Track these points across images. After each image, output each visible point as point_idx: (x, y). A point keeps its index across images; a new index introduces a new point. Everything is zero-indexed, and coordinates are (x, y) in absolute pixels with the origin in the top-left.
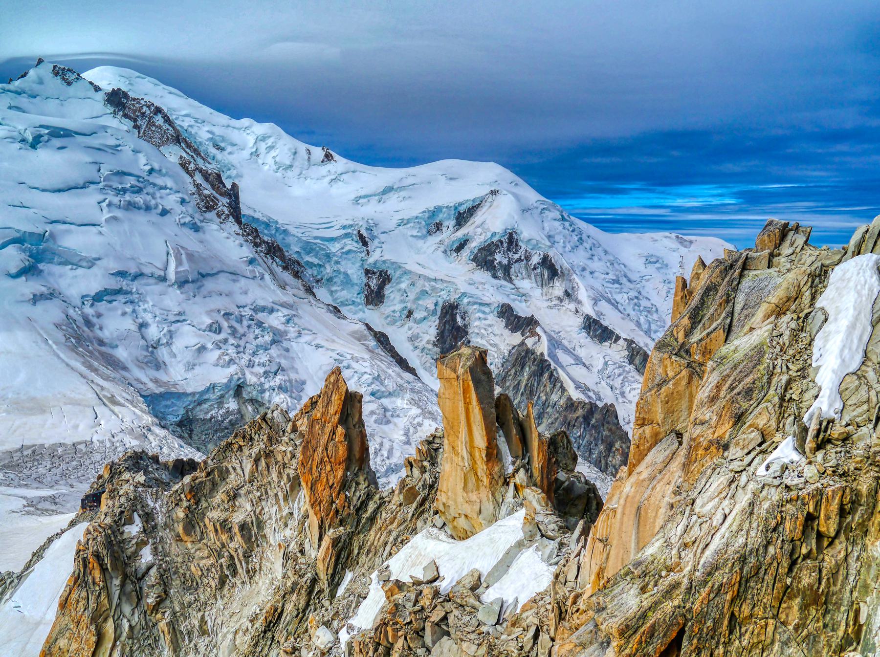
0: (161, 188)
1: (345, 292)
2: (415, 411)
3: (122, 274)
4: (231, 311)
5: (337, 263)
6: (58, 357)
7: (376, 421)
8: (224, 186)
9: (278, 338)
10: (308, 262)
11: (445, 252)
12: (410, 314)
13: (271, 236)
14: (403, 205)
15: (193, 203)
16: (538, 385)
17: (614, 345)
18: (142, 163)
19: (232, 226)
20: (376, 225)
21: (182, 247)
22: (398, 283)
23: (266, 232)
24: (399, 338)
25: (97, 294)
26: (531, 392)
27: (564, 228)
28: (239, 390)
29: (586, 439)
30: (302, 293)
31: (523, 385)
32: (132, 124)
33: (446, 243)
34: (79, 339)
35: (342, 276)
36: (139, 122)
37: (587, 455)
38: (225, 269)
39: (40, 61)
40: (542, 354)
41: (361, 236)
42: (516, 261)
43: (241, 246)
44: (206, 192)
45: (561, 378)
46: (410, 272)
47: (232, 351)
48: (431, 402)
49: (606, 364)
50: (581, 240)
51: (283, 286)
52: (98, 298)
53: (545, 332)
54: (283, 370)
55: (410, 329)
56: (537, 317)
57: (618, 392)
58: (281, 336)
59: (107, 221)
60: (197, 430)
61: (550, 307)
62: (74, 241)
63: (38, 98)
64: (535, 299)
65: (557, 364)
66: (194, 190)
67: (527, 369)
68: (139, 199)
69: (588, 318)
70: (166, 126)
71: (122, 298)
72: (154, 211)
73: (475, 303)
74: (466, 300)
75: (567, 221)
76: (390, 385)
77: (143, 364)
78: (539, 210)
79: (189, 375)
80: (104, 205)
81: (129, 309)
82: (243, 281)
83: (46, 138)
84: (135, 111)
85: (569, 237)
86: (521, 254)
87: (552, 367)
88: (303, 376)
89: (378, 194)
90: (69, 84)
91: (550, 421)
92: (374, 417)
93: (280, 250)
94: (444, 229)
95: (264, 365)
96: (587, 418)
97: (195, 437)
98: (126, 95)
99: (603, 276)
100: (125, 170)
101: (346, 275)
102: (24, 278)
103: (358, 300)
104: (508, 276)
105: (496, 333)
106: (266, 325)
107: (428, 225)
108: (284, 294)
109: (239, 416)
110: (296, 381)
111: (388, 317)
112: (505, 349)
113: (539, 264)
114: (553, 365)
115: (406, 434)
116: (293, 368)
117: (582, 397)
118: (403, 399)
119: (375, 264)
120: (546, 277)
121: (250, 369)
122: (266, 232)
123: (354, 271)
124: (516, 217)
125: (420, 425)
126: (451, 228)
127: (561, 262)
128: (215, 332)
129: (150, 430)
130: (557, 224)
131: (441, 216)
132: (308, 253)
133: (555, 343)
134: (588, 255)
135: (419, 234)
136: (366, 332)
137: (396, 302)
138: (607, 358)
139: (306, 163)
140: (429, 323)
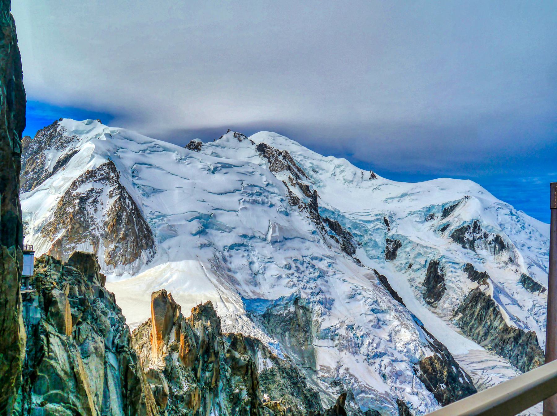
0: (272, 193)
1: (374, 251)
2: (396, 323)
3: (245, 236)
4: (298, 258)
5: (371, 235)
6: (206, 275)
7: (372, 326)
8: (310, 192)
9: (322, 275)
10: (354, 234)
11: (435, 231)
12: (410, 266)
13: (335, 218)
14: (413, 203)
15: (287, 201)
16: (486, 315)
17: (541, 294)
18: (264, 181)
19: (306, 214)
20: (395, 214)
21: (277, 224)
22: (405, 248)
23: (332, 216)
24: (399, 281)
25: (231, 246)
26: (481, 319)
27: (512, 220)
28: (296, 301)
29: (515, 353)
30: (340, 251)
31: (476, 314)
32: (268, 160)
33: (435, 226)
34: (218, 267)
35: (373, 242)
36: (271, 159)
37: (515, 362)
38: (299, 236)
39: (229, 131)
40: (489, 296)
41: (386, 220)
42: (478, 239)
43: (309, 224)
44: (294, 196)
45: (501, 312)
46: (412, 242)
47: (295, 280)
48: (407, 319)
49: (534, 305)
50: (523, 227)
51: (329, 247)
52: (231, 247)
53: (493, 282)
54: (322, 292)
55: (410, 275)
56: (489, 273)
57: (541, 324)
58: (324, 274)
59: (241, 209)
60: (272, 320)
61: (499, 268)
62: (225, 219)
63: (226, 148)
64: (489, 262)
65: (498, 302)
66: (288, 194)
67: (479, 304)
68: (259, 199)
69: (524, 276)
70: (283, 161)
71: (243, 248)
72: (266, 205)
73: (450, 262)
74: (444, 260)
75: (514, 215)
76: (384, 306)
77: (248, 283)
78: (496, 208)
79: (271, 291)
80: (241, 201)
81: (246, 254)
82: (308, 243)
83: (219, 168)
84: (269, 154)
85: (514, 226)
86: (482, 234)
87: (495, 305)
88: (333, 297)
89: (399, 197)
90: (241, 141)
91: (492, 338)
92: (372, 324)
93: (339, 226)
94: (435, 218)
95: (312, 289)
96: (516, 339)
97: (271, 324)
98: (266, 146)
99: (537, 250)
100: (255, 184)
101: (375, 242)
102: (198, 236)
103: (381, 256)
104: (472, 247)
105: (461, 281)
106: (316, 267)
107: (426, 215)
108: (330, 251)
109: (294, 315)
110: (329, 299)
111: (397, 267)
112: (467, 291)
113: (493, 241)
114: (496, 304)
115: (390, 336)
116: (329, 291)
117: (514, 325)
118: (390, 315)
119: (392, 236)
120: (497, 249)
121: (304, 290)
122: (332, 216)
123: (380, 240)
124: (479, 212)
125: (399, 331)
126: (440, 217)
127: (507, 240)
128: (288, 269)
129: (240, 317)
130: (507, 217)
131: (434, 210)
132: (355, 229)
133: (499, 290)
134: (528, 237)
135: (420, 220)
136: (374, 275)
137: (403, 258)
138: (535, 302)
139: (361, 180)
140: (422, 272)
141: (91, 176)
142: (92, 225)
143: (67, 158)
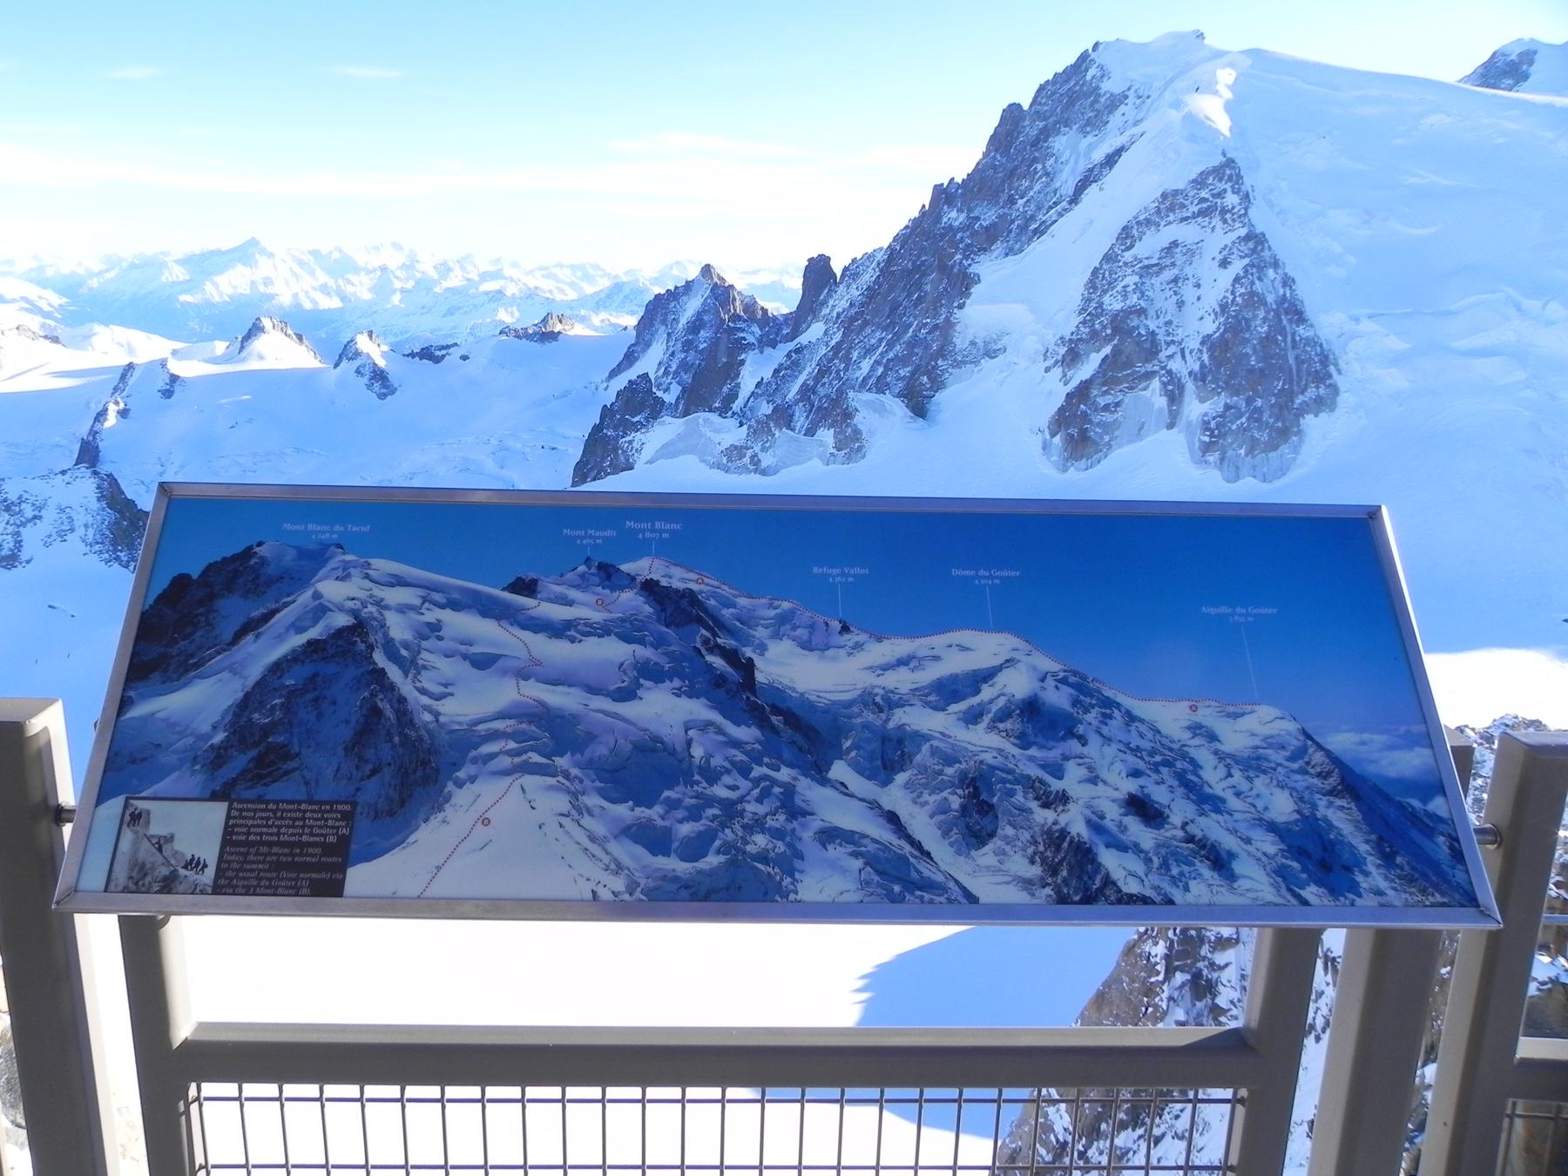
141: (1171, 209)
142: (1168, 344)
143: (1111, 160)
